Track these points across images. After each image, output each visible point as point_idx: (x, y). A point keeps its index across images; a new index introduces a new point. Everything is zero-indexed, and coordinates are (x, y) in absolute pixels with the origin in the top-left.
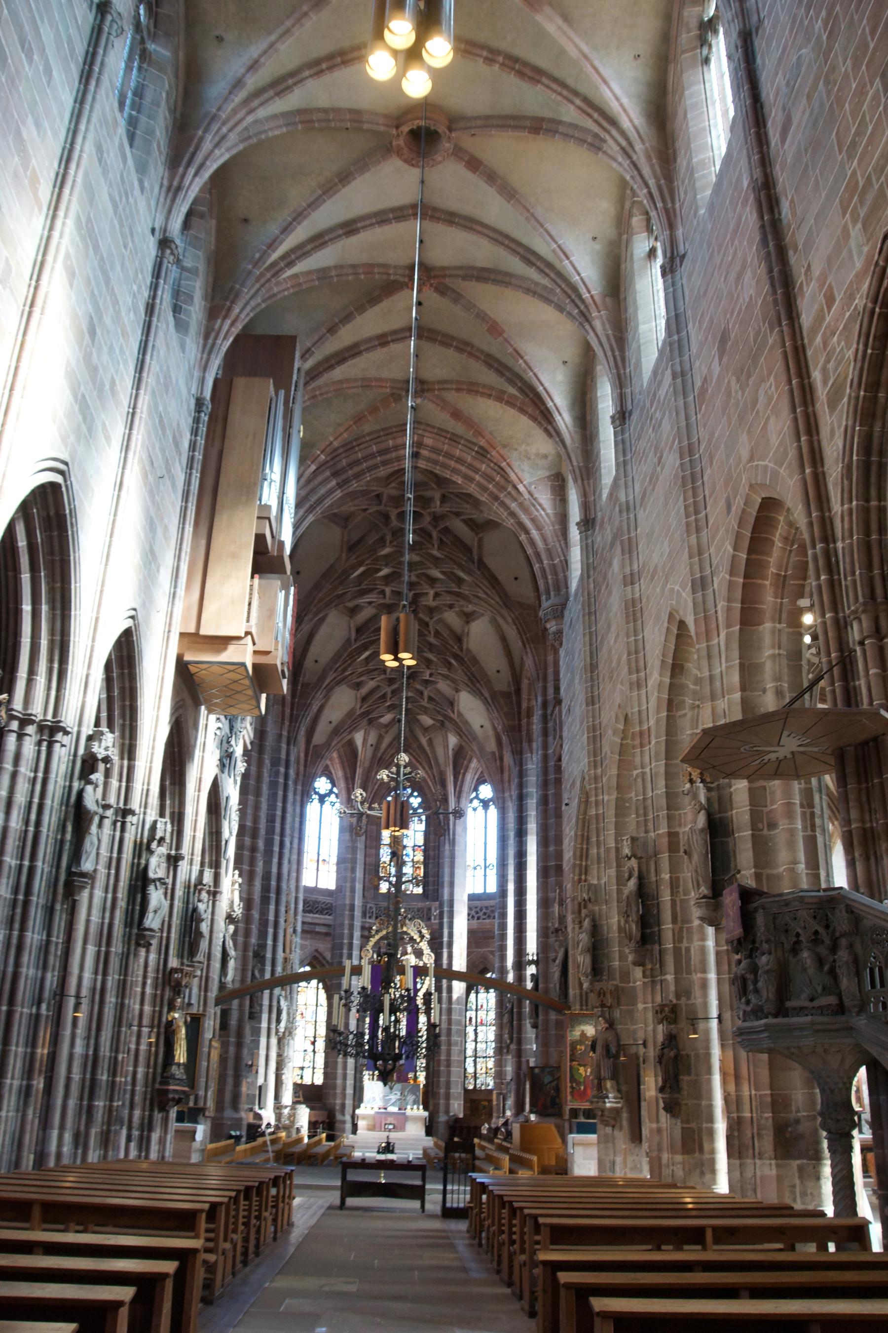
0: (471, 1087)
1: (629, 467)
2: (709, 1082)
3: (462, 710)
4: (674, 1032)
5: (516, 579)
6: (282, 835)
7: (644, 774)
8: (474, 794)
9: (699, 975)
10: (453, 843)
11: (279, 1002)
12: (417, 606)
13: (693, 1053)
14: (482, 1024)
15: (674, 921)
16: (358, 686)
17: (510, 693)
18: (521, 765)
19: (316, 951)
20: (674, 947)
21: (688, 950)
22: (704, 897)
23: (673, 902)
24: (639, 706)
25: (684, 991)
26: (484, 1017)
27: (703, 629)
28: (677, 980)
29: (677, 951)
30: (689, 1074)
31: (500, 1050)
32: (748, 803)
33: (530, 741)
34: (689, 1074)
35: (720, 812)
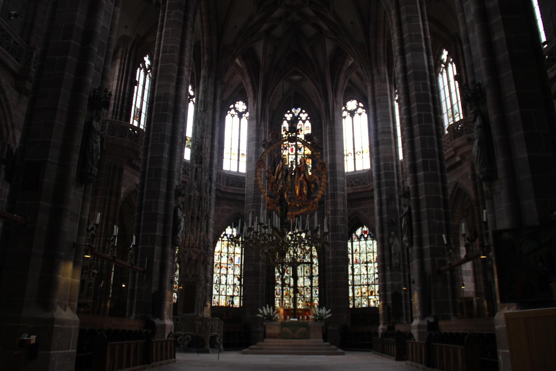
8: (343, 108)
14: (357, 263)
26: (358, 257)
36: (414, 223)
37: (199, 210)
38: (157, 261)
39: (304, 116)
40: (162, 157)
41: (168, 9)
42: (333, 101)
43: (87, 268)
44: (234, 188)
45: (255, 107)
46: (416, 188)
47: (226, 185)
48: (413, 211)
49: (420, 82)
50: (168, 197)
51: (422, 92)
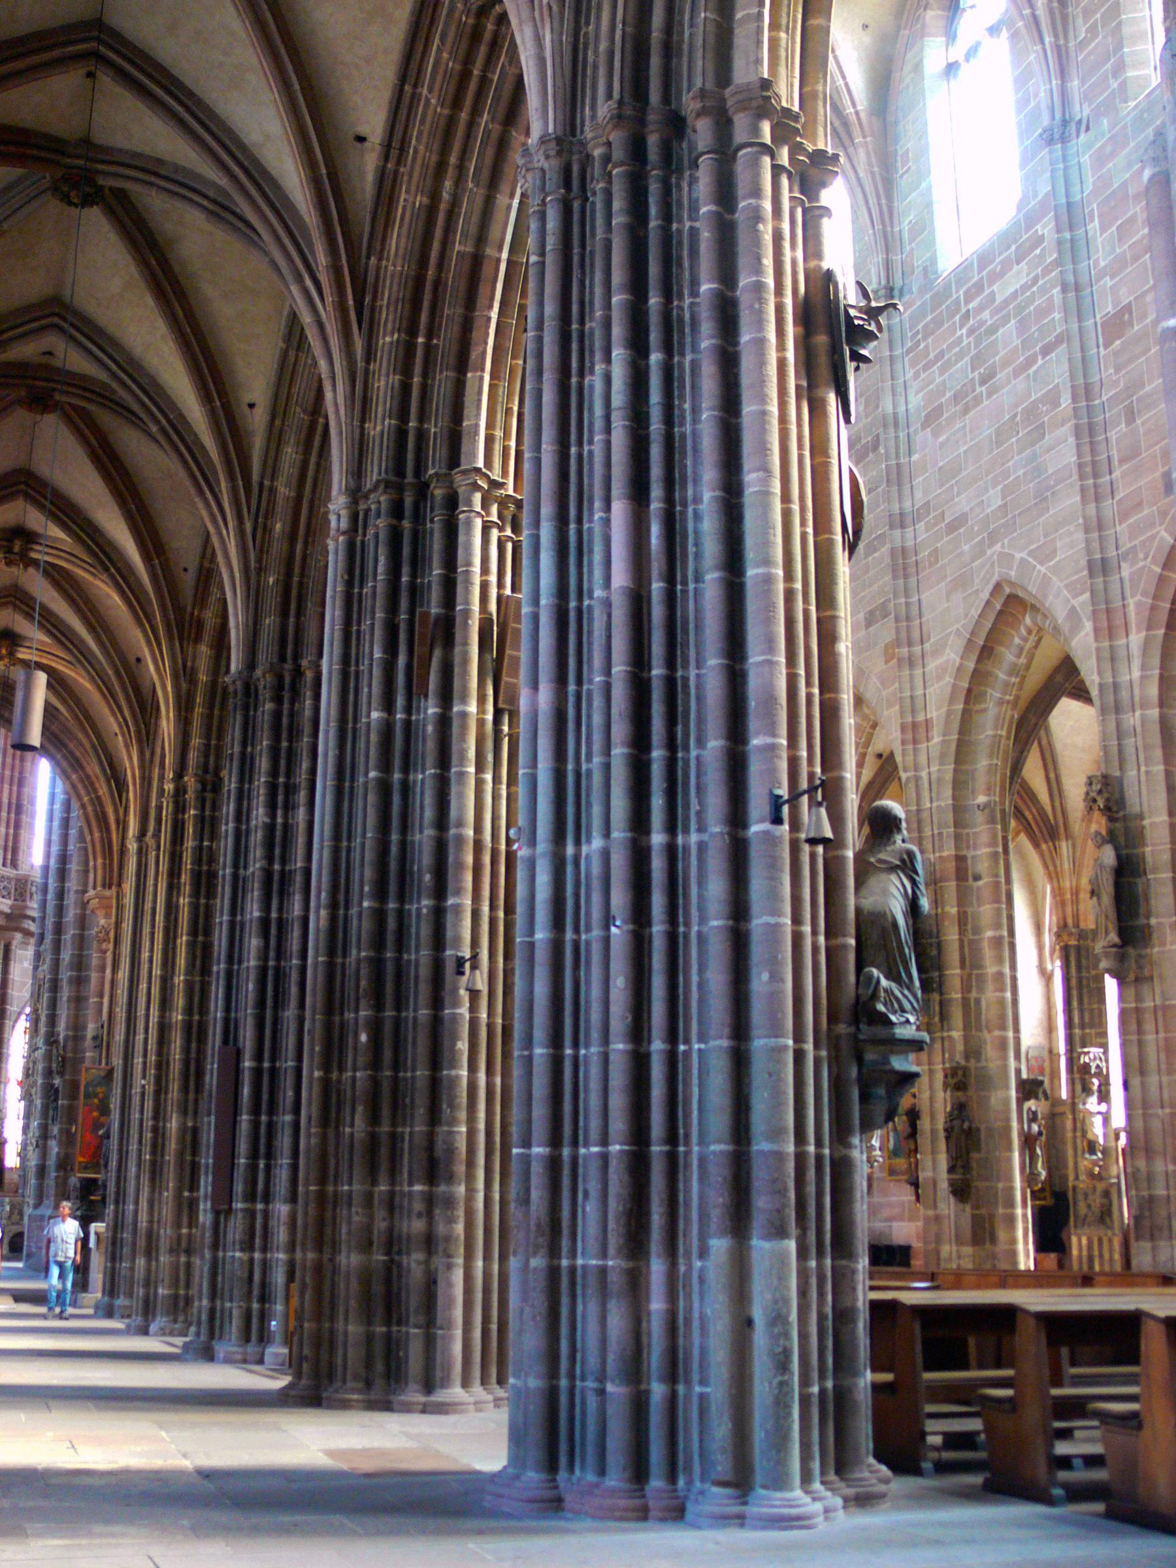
1: (898, 367)
2: (1009, 1160)
4: (963, 1100)
7: (917, 779)
9: (997, 1033)
13: (982, 1127)
15: (962, 967)
20: (963, 998)
21: (978, 1001)
22: (1114, 946)
23: (961, 941)
24: (912, 689)
25: (973, 1051)
27: (1105, 624)
28: (966, 1039)
29: (965, 1002)
30: (979, 1151)
32: (1168, 840)
34: (979, 1151)
35: (1127, 847)
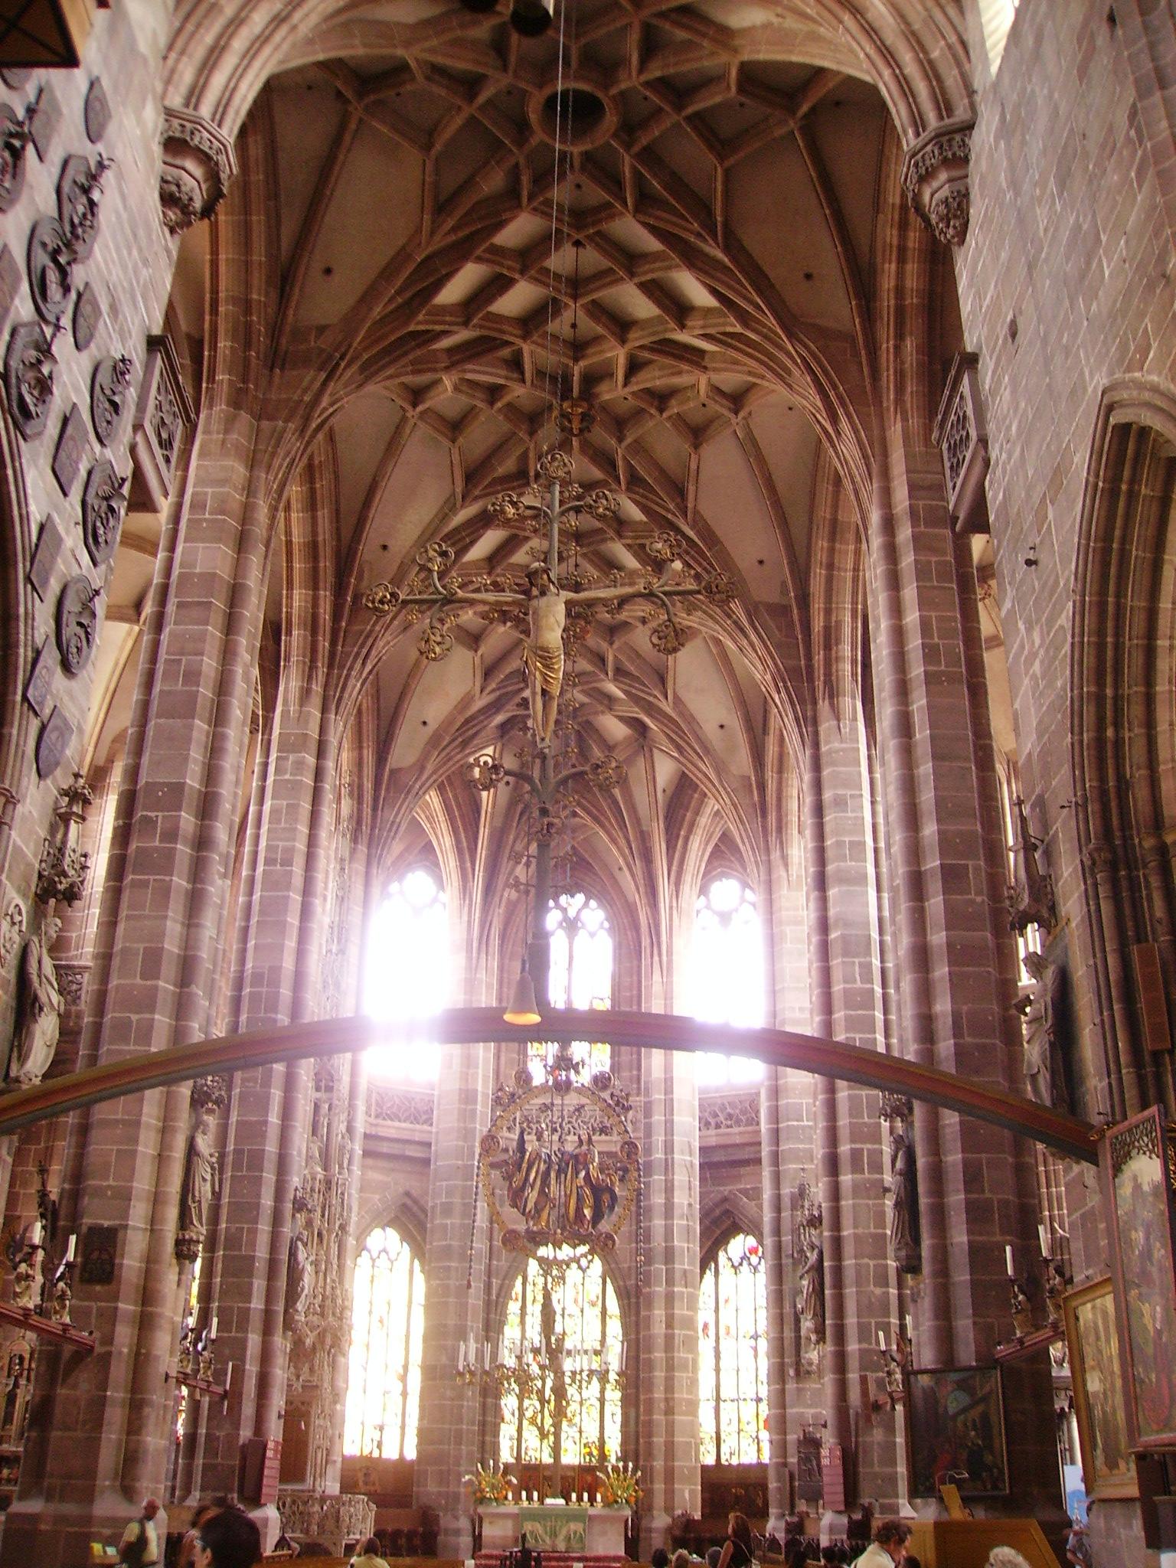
0: (709, 1460)
3: (681, 693)
5: (808, 277)
6: (307, 891)
10: (668, 970)
11: (293, 1254)
12: (591, 407)
16: (474, 640)
17: (785, 610)
18: (816, 745)
19: (408, 1194)
31: (788, 1364)
33: (833, 693)
36: (827, 1292)
37: (323, 1216)
38: (252, 1368)
39: (594, 915)
40: (266, 1122)
41: (279, 751)
42: (671, 908)
43: (21, 1358)
44: (397, 1124)
45: (465, 918)
46: (836, 1212)
47: (377, 1117)
48: (826, 1264)
49: (857, 960)
50: (277, 1219)
51: (859, 985)
